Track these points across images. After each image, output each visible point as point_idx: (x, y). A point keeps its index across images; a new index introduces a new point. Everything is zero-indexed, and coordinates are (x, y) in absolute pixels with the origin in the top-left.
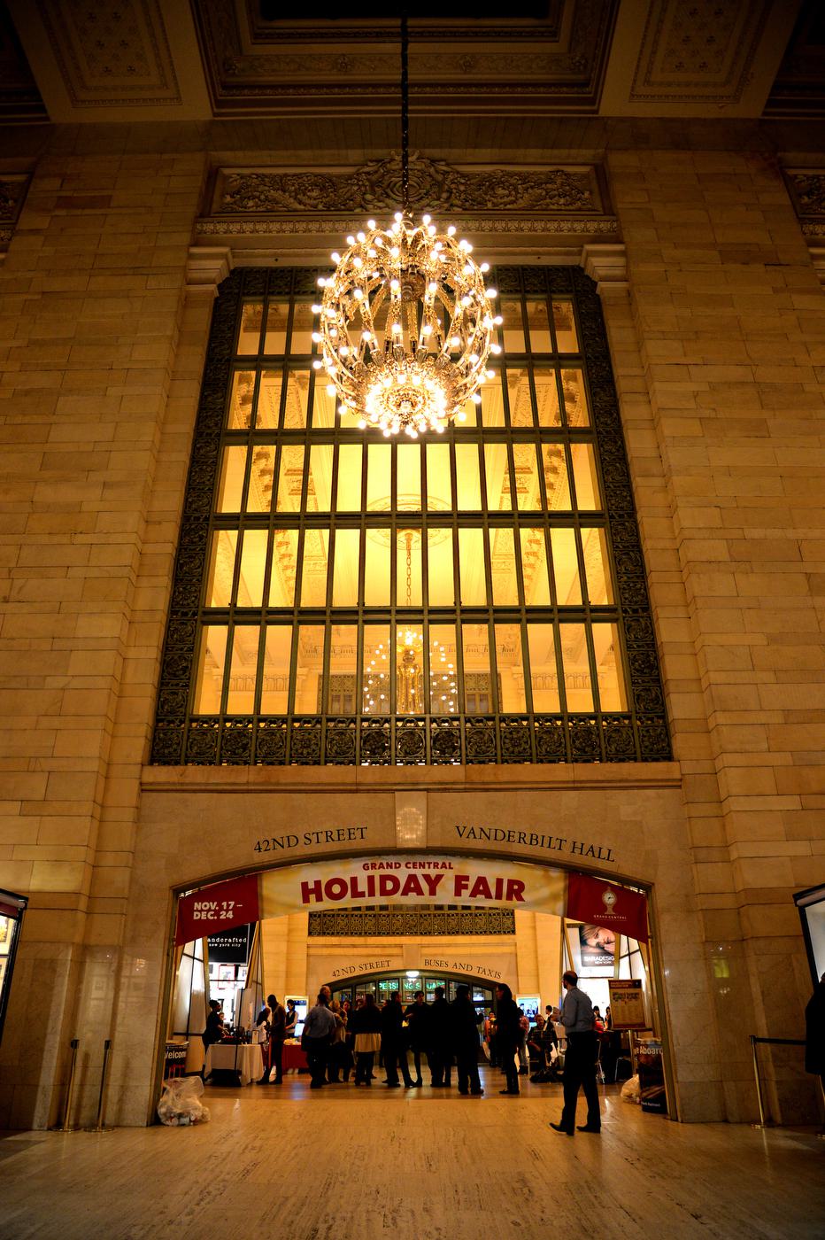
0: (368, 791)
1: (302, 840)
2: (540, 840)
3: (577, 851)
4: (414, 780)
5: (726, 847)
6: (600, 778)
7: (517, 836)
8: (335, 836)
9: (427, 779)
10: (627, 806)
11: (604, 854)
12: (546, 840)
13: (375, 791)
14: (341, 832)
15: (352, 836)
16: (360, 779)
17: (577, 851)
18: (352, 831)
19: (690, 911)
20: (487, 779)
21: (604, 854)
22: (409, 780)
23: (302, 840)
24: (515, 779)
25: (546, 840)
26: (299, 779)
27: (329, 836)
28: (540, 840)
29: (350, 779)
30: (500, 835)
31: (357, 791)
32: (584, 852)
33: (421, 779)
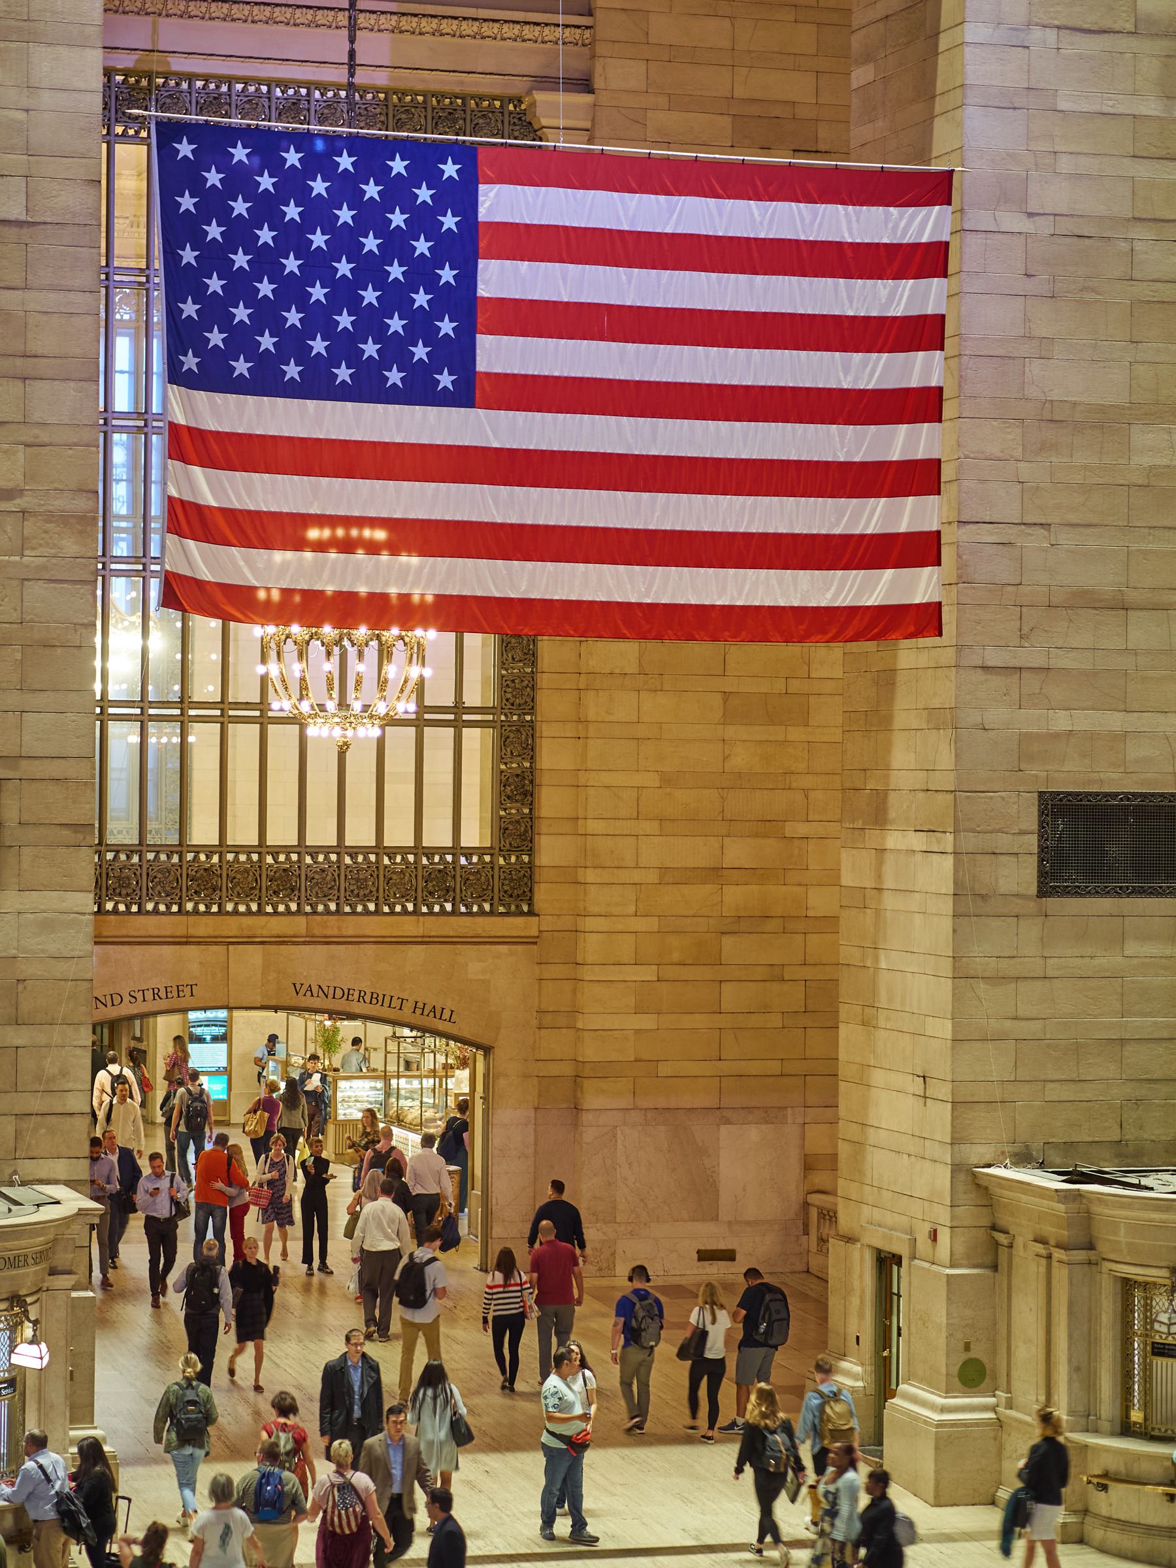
0: (199, 943)
1: (127, 998)
2: (380, 999)
3: (418, 1011)
4: (250, 933)
5: (575, 1012)
6: (451, 934)
7: (356, 994)
8: (162, 994)
9: (265, 933)
10: (475, 964)
11: (446, 1015)
12: (387, 999)
13: (206, 943)
14: (169, 989)
15: (181, 994)
16: (192, 932)
17: (418, 1011)
18: (181, 988)
19: (526, 1076)
20: (329, 932)
21: (446, 1015)
22: (246, 933)
23: (127, 998)
24: (361, 933)
25: (387, 999)
26: (124, 932)
27: (156, 994)
28: (380, 999)
29: (181, 931)
30: (339, 993)
31: (186, 943)
32: (426, 1013)
33: (259, 932)
